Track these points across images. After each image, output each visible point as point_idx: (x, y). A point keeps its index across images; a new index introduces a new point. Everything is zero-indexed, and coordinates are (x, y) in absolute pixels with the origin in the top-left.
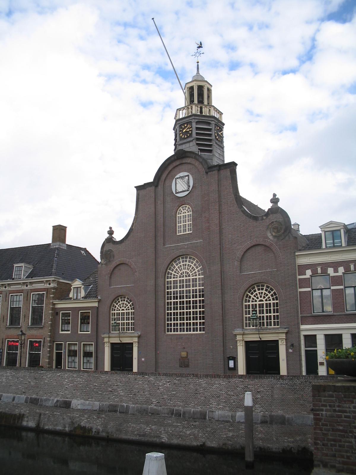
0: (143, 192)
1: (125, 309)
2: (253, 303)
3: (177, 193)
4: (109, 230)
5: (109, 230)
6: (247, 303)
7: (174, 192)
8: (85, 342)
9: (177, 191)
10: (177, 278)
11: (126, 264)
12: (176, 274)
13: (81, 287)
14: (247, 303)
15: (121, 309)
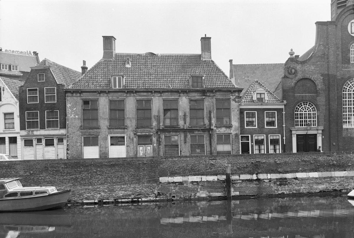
0: (325, 27)
1: (307, 111)
2: (300, 112)
3: (352, 33)
4: (290, 51)
5: (290, 51)
6: (297, 113)
7: (350, 33)
8: (271, 134)
9: (352, 32)
10: (351, 92)
11: (307, 79)
12: (350, 89)
13: (264, 93)
14: (297, 113)
15: (304, 111)
